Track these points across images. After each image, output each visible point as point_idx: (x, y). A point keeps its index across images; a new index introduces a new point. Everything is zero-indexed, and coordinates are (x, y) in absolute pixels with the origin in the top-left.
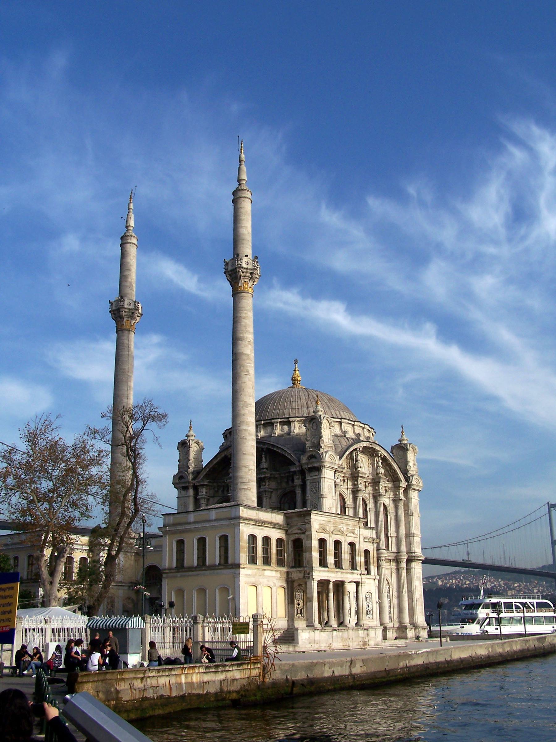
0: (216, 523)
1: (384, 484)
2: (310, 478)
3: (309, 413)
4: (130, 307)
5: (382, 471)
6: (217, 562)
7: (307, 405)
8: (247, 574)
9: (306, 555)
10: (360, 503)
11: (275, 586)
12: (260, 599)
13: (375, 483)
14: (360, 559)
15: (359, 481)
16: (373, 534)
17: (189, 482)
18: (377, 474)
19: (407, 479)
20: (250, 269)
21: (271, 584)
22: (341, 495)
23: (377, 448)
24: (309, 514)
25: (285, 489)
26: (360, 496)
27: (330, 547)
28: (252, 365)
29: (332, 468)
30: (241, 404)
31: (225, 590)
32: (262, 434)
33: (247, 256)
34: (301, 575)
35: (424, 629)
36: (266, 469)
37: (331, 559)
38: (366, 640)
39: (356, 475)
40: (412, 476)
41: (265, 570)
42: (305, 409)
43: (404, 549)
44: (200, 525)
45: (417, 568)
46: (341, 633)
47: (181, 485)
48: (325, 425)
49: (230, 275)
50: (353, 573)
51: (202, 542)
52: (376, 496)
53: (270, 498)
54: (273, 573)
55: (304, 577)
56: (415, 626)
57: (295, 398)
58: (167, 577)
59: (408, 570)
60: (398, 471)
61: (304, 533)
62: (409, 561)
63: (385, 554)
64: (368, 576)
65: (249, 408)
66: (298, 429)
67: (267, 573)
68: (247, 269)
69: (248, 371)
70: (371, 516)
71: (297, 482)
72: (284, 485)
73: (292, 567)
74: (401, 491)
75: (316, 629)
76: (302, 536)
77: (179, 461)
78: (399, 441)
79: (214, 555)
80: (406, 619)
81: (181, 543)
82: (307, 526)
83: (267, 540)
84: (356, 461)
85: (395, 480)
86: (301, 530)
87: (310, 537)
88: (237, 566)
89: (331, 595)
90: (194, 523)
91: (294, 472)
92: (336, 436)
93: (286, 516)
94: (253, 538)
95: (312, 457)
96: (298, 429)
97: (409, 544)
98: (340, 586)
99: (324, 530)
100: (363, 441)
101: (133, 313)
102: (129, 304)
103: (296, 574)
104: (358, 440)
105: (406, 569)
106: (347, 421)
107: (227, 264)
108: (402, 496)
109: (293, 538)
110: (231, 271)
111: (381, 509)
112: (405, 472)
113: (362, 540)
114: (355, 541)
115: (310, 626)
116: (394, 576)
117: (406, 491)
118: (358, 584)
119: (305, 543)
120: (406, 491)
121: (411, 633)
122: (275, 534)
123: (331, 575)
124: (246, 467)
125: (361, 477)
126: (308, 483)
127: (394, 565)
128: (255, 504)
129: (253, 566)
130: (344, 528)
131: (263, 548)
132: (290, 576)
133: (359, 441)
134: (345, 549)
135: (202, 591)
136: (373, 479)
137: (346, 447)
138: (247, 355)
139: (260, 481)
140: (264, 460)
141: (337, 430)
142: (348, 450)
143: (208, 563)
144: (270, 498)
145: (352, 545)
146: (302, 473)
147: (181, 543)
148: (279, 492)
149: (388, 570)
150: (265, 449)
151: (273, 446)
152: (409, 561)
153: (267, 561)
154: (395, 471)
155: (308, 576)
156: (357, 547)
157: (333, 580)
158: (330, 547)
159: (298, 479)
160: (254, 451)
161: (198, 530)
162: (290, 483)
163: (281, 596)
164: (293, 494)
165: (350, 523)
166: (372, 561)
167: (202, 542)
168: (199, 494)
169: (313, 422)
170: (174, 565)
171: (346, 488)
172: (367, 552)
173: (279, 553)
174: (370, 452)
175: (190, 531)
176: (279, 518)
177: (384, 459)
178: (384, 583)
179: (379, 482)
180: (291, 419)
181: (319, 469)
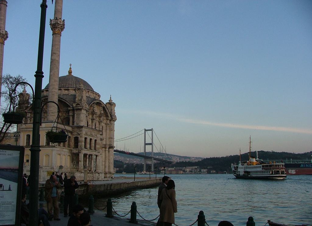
2: (76, 113)
3: (76, 86)
4: (3, 33)
5: (102, 112)
6: (45, 144)
11: (67, 155)
13: (100, 117)
14: (97, 146)
15: (94, 116)
20: (61, 25)
23: (102, 103)
26: (94, 121)
27: (88, 141)
29: (86, 110)
37: (88, 146)
38: (99, 177)
39: (93, 113)
40: (113, 115)
41: (63, 149)
42: (75, 85)
48: (84, 92)
49: (52, 26)
50: (96, 152)
54: (66, 150)
56: (110, 173)
57: (70, 80)
60: (108, 113)
61: (79, 135)
62: (109, 148)
66: (72, 92)
67: (64, 150)
68: (60, 24)
71: (71, 114)
72: (64, 115)
73: (73, 148)
74: (108, 122)
76: (79, 136)
78: (109, 101)
84: (94, 107)
86: (77, 133)
87: (81, 137)
89: (88, 160)
91: (70, 110)
92: (87, 97)
95: (78, 104)
106: (91, 91)
110: (53, 24)
113: (99, 139)
114: (97, 139)
117: (110, 120)
118: (97, 156)
119: (80, 139)
120: (110, 120)
123: (88, 152)
125: (95, 114)
126: (75, 115)
127: (104, 149)
132: (72, 151)
134: (93, 141)
136: (99, 115)
137: (91, 102)
145: (96, 140)
146: (73, 110)
148: (62, 117)
151: (61, 98)
152: (109, 148)
156: (97, 142)
157: (89, 154)
158: (88, 141)
159: (71, 113)
162: (67, 114)
163: (68, 159)
165: (96, 132)
168: (28, 116)
179: (101, 117)
180: (69, 88)
181: (80, 110)
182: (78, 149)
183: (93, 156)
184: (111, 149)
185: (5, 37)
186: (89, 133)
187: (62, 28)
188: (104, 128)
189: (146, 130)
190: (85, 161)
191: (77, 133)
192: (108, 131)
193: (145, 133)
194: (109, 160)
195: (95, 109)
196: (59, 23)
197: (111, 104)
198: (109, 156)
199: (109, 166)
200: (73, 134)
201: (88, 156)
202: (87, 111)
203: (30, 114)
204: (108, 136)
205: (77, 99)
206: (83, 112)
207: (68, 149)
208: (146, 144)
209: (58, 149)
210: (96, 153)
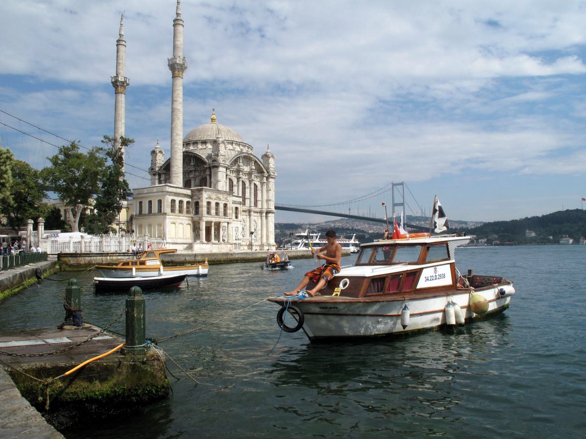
0: (156, 194)
5: (254, 167)
7: (216, 133)
8: (169, 219)
10: (241, 183)
12: (177, 229)
16: (241, 200)
17: (156, 172)
18: (251, 169)
19: (268, 172)
21: (183, 222)
22: (230, 179)
23: (252, 156)
24: (201, 190)
25: (202, 176)
26: (241, 180)
27: (213, 205)
28: (182, 115)
30: (174, 134)
33: (179, 57)
34: (198, 219)
35: (274, 246)
36: (193, 166)
37: (213, 211)
43: (265, 206)
44: (149, 195)
46: (217, 246)
47: (152, 173)
51: (150, 202)
52: (250, 182)
53: (195, 180)
54: (184, 218)
55: (199, 220)
56: (269, 245)
58: (135, 219)
59: (266, 217)
62: (267, 213)
64: (237, 220)
65: (179, 137)
67: (180, 217)
69: (179, 118)
70: (247, 191)
71: (208, 173)
72: (202, 174)
73: (195, 215)
74: (265, 178)
75: (221, 244)
76: (199, 200)
77: (152, 161)
79: (155, 209)
80: (264, 241)
81: (141, 203)
82: (201, 196)
83: (181, 202)
87: (202, 201)
90: (147, 193)
92: (229, 149)
93: (192, 191)
94: (173, 201)
97: (268, 204)
98: (218, 225)
100: (244, 153)
101: (124, 84)
102: (121, 79)
104: (241, 152)
105: (266, 217)
107: (169, 60)
109: (195, 201)
110: (171, 65)
111: (253, 186)
112: (268, 169)
113: (231, 202)
116: (260, 220)
117: (267, 178)
118: (228, 223)
119: (200, 204)
120: (267, 178)
121: (266, 248)
122: (185, 200)
123: (214, 219)
124: (177, 166)
126: (212, 173)
127: (259, 214)
128: (181, 185)
129: (173, 214)
131: (179, 206)
135: (150, 225)
138: (179, 109)
139: (185, 173)
140: (192, 161)
143: (152, 212)
144: (195, 180)
145: (225, 205)
146: (210, 168)
147: (141, 203)
149: (255, 217)
150: (188, 157)
154: (262, 168)
155: (200, 219)
157: (214, 221)
158: (213, 205)
160: (181, 158)
161: (148, 197)
164: (206, 178)
166: (239, 212)
167: (150, 202)
169: (215, 143)
170: (138, 213)
171: (233, 176)
172: (237, 208)
173: (188, 208)
175: (145, 197)
176: (188, 192)
177: (256, 162)
178: (253, 223)
181: (217, 167)
182: (198, 216)
183: (221, 224)
184: (270, 215)
185: (125, 84)
187: (183, 68)
189: (394, 185)
190: (208, 230)
191: (198, 197)
192: (265, 192)
193: (393, 188)
194: (267, 228)
195: (241, 164)
196: (178, 62)
197: (266, 156)
199: (267, 236)
200: (193, 198)
201: (213, 224)
202: (227, 168)
203: (164, 176)
204: (265, 198)
206: (221, 169)
207: (186, 217)
208: (395, 205)
209: (172, 217)
210: (227, 219)
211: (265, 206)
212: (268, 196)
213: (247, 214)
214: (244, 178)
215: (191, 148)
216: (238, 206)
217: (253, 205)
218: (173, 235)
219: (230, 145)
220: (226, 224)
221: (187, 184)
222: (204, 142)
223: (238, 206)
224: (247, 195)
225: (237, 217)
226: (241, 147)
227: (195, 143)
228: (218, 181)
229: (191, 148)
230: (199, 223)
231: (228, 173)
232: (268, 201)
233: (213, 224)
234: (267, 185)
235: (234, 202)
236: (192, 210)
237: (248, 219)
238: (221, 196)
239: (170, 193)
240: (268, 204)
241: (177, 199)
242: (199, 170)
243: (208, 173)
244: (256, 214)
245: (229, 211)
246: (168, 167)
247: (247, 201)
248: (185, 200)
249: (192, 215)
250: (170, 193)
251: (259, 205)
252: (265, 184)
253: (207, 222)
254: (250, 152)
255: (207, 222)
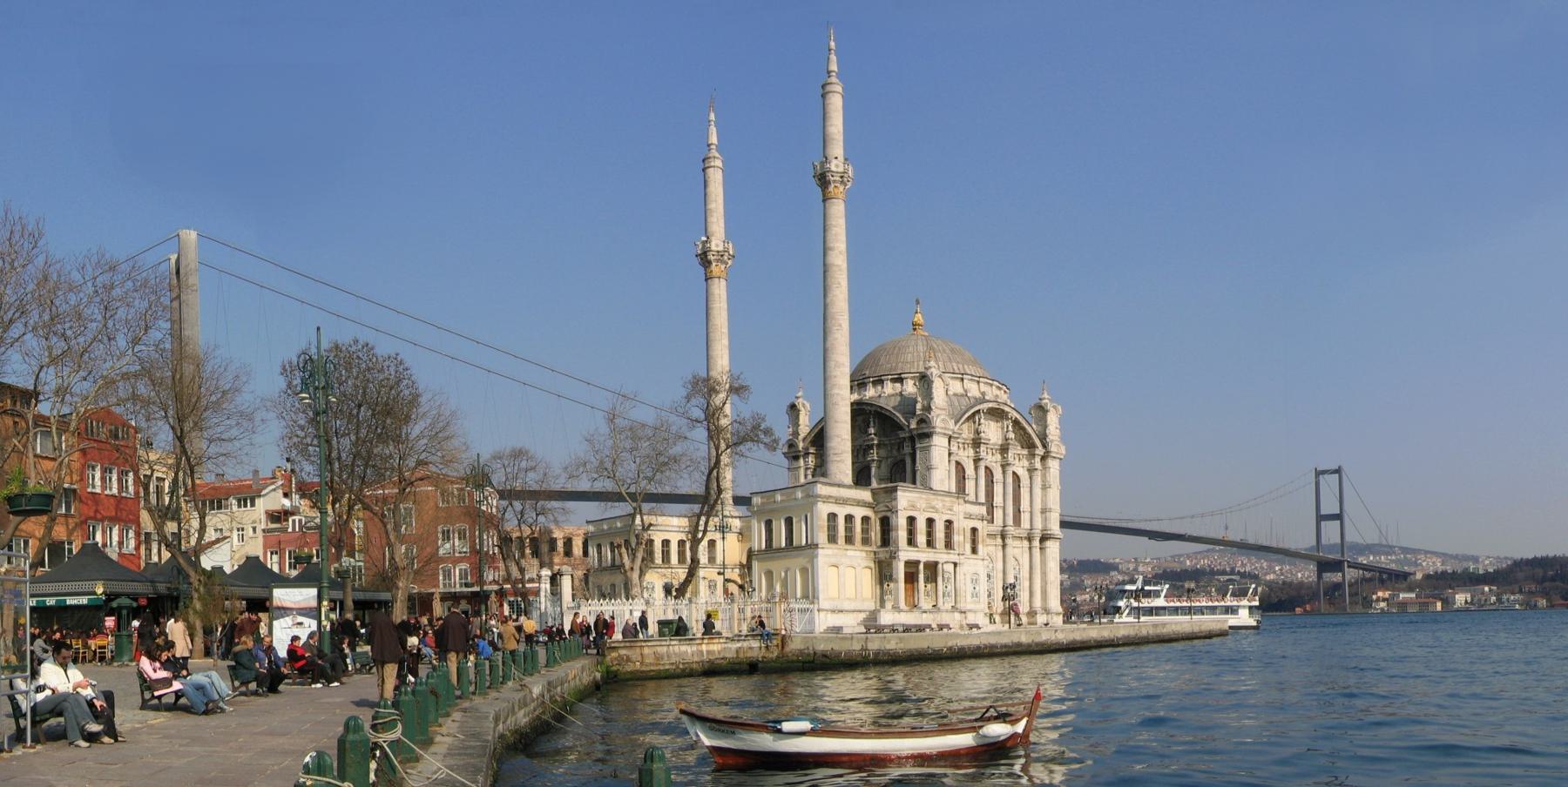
1: (1016, 450)
5: (1011, 435)
8: (826, 555)
9: (893, 534)
10: (982, 472)
13: (1004, 449)
16: (983, 510)
19: (1044, 446)
22: (958, 463)
23: (1007, 409)
24: (895, 490)
26: (982, 465)
27: (921, 525)
30: (831, 364)
31: (804, 571)
32: (856, 397)
37: (921, 538)
43: (1038, 525)
45: (1053, 548)
56: (1047, 611)
62: (1044, 539)
63: (1011, 530)
66: (910, 387)
70: (998, 489)
71: (907, 450)
74: (1038, 459)
80: (1038, 603)
85: (1030, 446)
88: (813, 546)
93: (874, 493)
96: (910, 387)
97: (1045, 520)
98: (932, 567)
99: (913, 507)
103: (883, 554)
108: (1038, 465)
111: (1010, 479)
112: (1043, 438)
115: (896, 608)
116: (1027, 555)
117: (1043, 458)
118: (955, 564)
119: (893, 521)
120: (1043, 458)
121: (1041, 619)
122: (859, 513)
123: (923, 555)
127: (1026, 543)
128: (849, 480)
130: (939, 505)
133: (984, 401)
141: (956, 387)
142: (971, 413)
145: (949, 523)
146: (912, 439)
149: (1017, 549)
150: (862, 414)
152: (1044, 539)
153: (849, 540)
155: (893, 556)
156: (955, 525)
158: (921, 525)
160: (848, 418)
163: (867, 578)
164: (903, 461)
169: (924, 380)
171: (966, 456)
172: (974, 530)
173: (865, 531)
174: (997, 414)
176: (866, 495)
177: (1016, 423)
178: (1011, 563)
181: (928, 436)
184: (1049, 543)
186: (922, 504)
188: (1025, 481)
192: (1038, 491)
195: (982, 428)
198: (1044, 563)
204: (1038, 506)
205: (919, 406)
209: (829, 552)
211: (1038, 525)
212: (1044, 501)
213: (999, 541)
214: (992, 459)
215: (870, 392)
216: (978, 524)
217: (1010, 521)
218: (833, 592)
219: (958, 383)
220: (950, 568)
221: (861, 477)
222: (900, 380)
223: (978, 524)
224: (998, 500)
225: (974, 551)
226: (983, 388)
227: (879, 382)
228: (929, 468)
229: (870, 392)
230: (890, 565)
231: (954, 449)
232: (1044, 511)
233: (921, 567)
234: (1044, 476)
235: (969, 517)
236: (875, 533)
237: (1000, 554)
238: (938, 503)
239: (827, 499)
240: (1045, 520)
241: (842, 512)
242: (891, 443)
243: (907, 450)
244: (1017, 543)
245: (957, 538)
246: (819, 438)
247: (998, 514)
248: (859, 513)
249: (874, 548)
250: (827, 499)
251: (1025, 524)
252: (1039, 473)
253: (908, 563)
254: (1004, 397)
255: (908, 563)
